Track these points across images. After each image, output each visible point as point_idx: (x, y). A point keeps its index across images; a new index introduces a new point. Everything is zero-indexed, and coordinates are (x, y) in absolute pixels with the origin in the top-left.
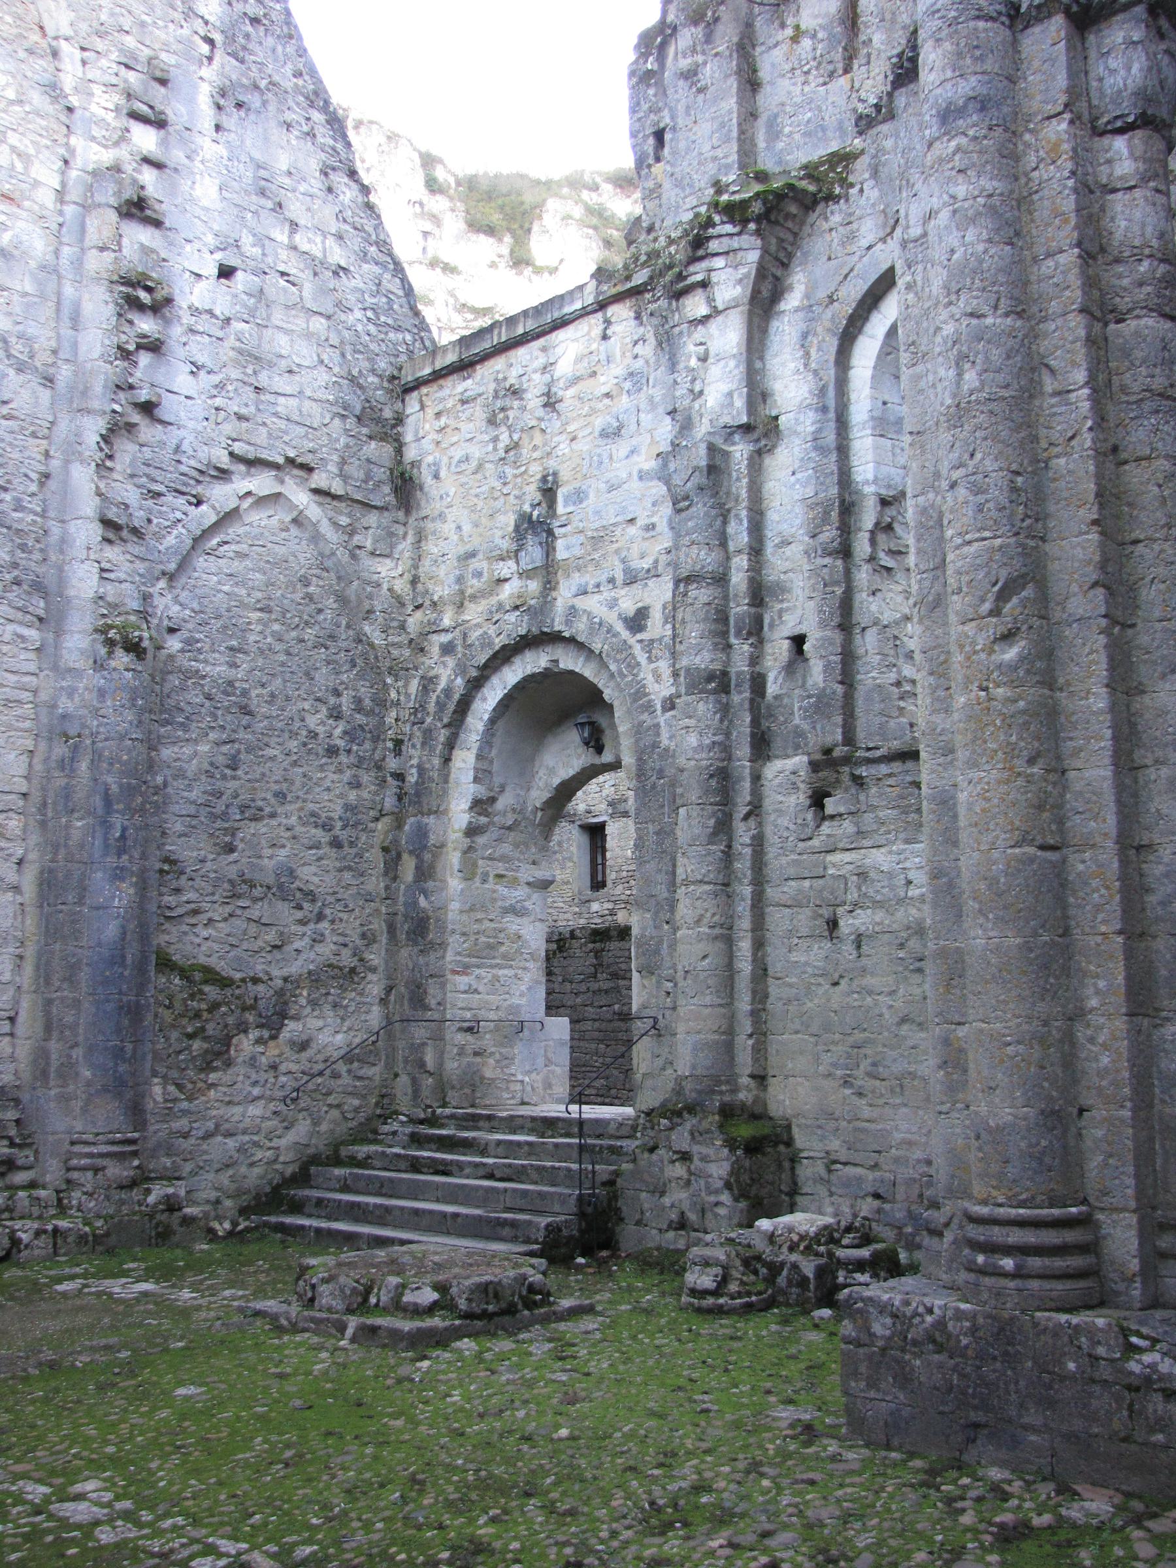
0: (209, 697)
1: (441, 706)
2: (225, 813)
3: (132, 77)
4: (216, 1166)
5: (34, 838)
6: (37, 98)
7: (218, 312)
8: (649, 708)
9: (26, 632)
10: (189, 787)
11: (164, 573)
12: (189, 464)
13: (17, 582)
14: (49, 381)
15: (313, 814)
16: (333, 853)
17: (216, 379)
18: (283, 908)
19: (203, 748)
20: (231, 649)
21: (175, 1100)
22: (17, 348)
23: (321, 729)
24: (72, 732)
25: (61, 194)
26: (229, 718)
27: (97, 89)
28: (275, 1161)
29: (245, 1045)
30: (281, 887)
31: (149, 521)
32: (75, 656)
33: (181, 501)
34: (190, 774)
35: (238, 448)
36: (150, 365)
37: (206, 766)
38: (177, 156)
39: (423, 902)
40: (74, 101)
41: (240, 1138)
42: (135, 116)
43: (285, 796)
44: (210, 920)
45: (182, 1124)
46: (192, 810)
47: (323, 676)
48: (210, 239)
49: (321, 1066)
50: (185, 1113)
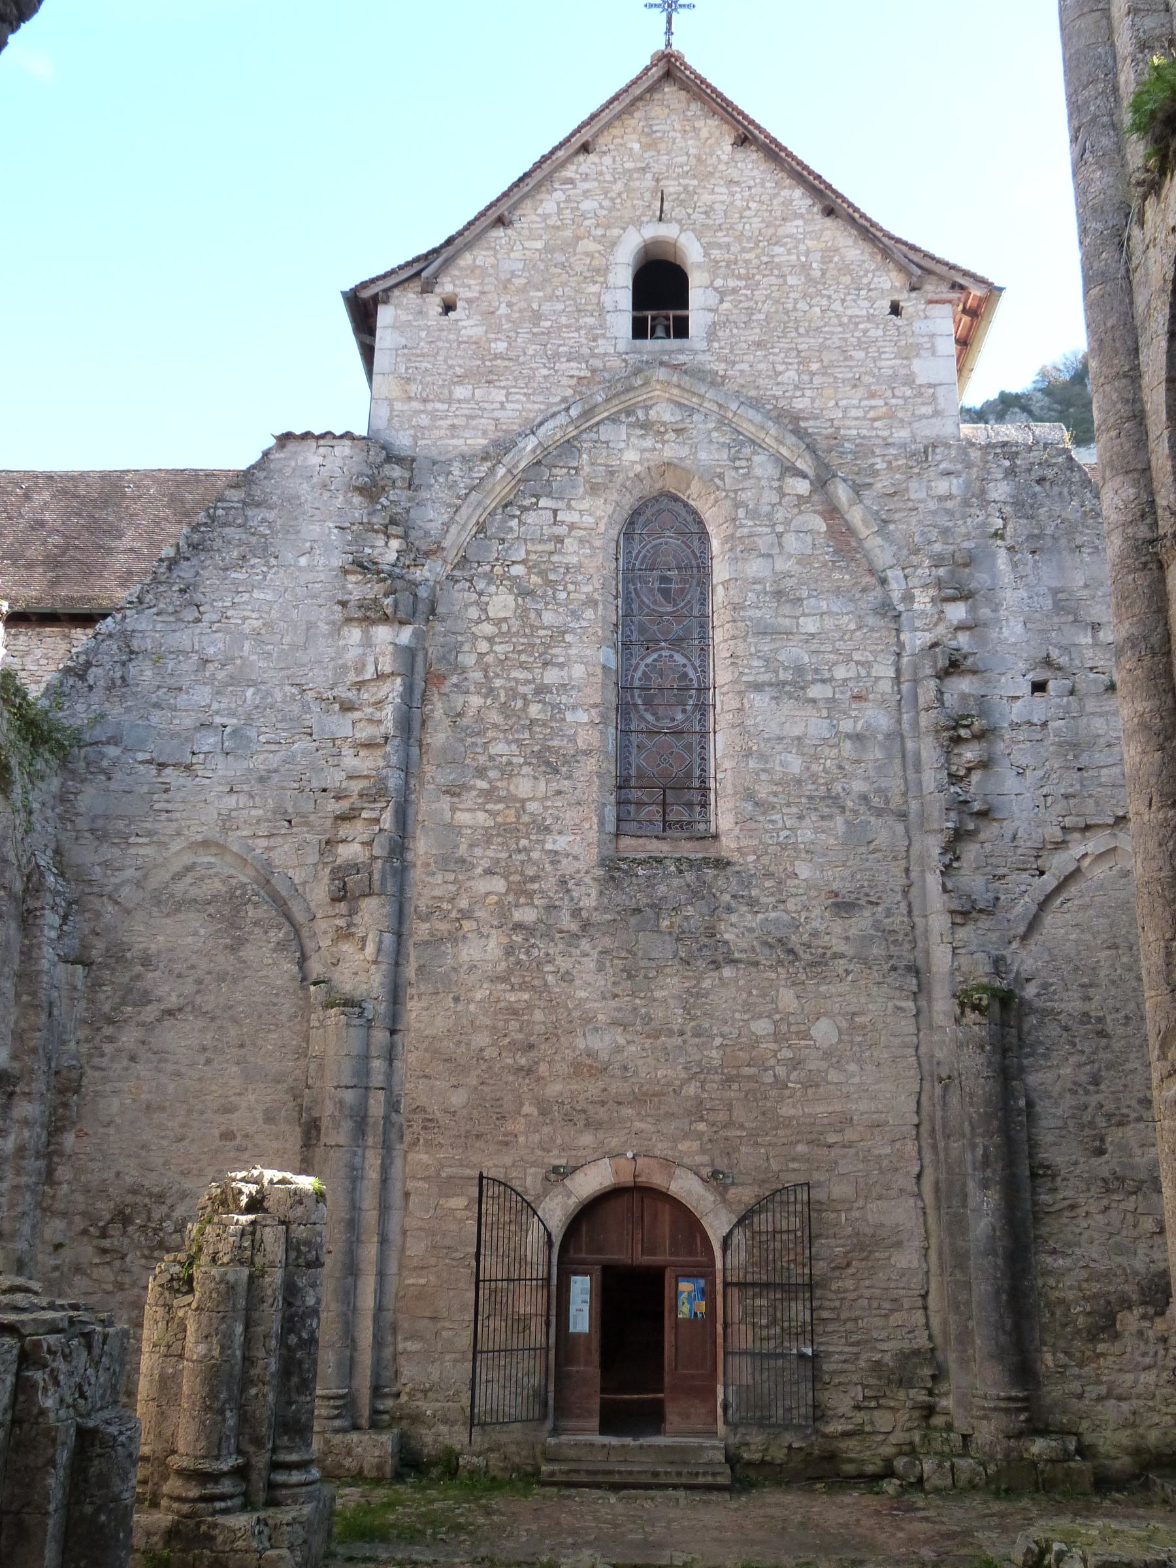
0: (1066, 1029)
3: (941, 572)
5: (928, 1156)
6: (871, 620)
7: (1035, 720)
9: (903, 1004)
10: (1056, 1104)
12: (1026, 844)
13: (894, 968)
14: (903, 816)
17: (1041, 773)
19: (1066, 1071)
20: (1082, 986)
21: (1065, 1366)
22: (876, 801)
24: (944, 1076)
25: (897, 680)
27: (917, 592)
31: (997, 899)
32: (942, 1016)
33: (1025, 875)
34: (1055, 1094)
35: (1068, 821)
36: (981, 780)
37: (1069, 1085)
38: (985, 612)
40: (901, 608)
41: (1134, 1402)
42: (946, 600)
45: (1075, 1386)
46: (1060, 1123)
48: (1022, 666)
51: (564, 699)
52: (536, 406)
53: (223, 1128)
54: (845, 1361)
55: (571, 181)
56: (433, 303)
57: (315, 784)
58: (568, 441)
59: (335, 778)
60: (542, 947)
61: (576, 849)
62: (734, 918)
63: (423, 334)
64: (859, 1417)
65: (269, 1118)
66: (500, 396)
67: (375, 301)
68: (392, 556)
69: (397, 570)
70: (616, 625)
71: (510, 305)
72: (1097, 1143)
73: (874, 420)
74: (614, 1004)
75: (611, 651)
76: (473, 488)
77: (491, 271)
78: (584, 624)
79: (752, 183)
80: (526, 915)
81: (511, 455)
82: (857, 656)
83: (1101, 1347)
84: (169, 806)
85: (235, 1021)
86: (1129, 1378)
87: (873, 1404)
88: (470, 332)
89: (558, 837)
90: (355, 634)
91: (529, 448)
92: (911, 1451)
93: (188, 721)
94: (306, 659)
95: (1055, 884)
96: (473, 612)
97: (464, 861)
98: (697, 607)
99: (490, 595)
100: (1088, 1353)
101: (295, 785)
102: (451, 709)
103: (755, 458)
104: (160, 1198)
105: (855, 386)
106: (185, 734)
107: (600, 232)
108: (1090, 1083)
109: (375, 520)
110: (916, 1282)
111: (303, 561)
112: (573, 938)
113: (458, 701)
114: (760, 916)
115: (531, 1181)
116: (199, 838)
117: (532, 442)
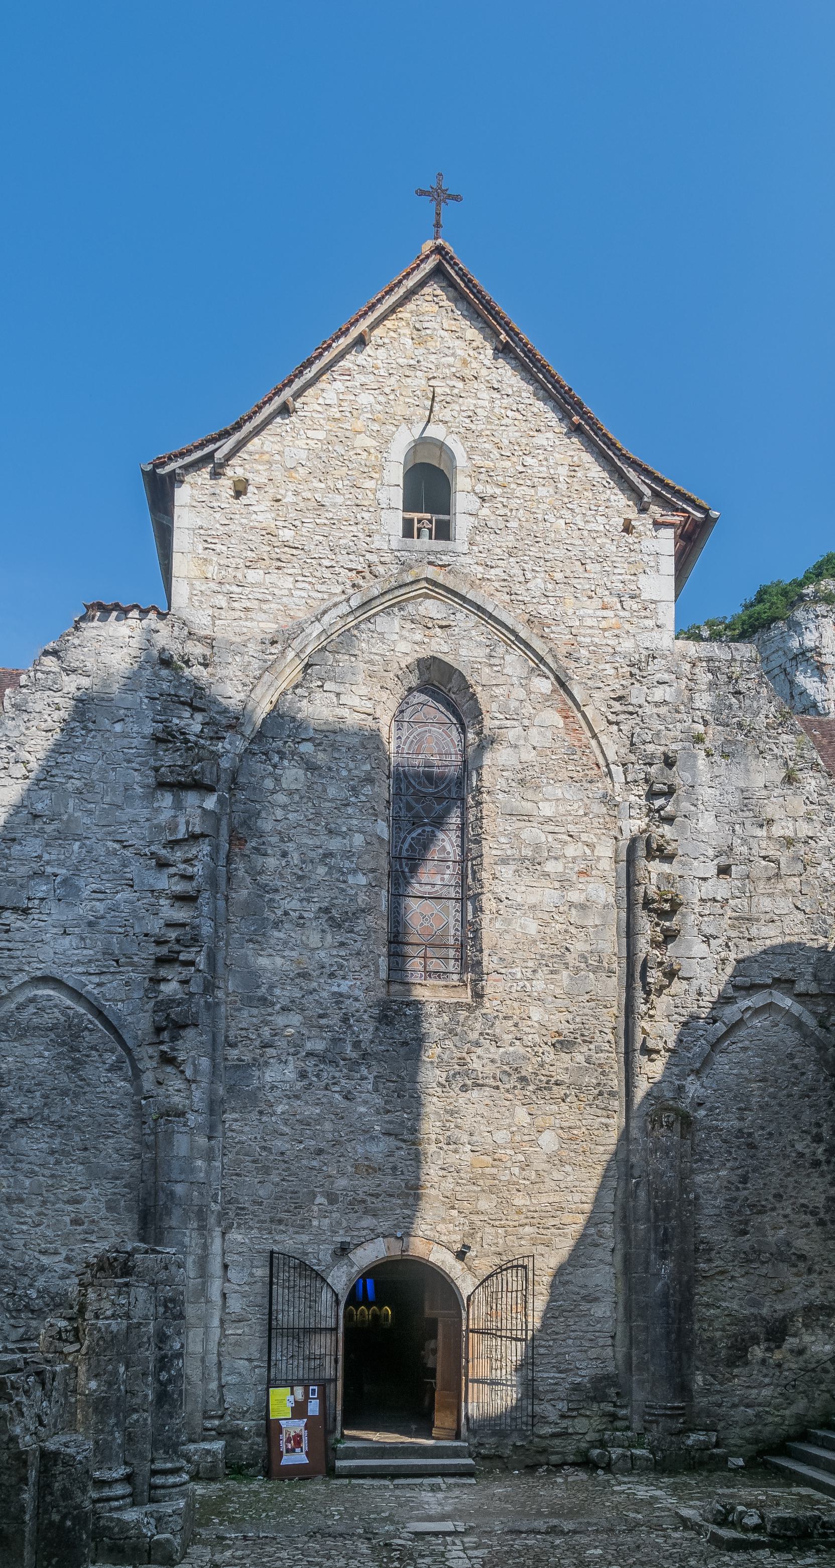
0: (725, 1141)
2: (739, 1211)
4: (741, 1424)
5: (619, 1237)
7: (719, 898)
10: (715, 1198)
11: (692, 1071)
15: (803, 1205)
16: (818, 1229)
18: (783, 1267)
20: (739, 1109)
23: (807, 1151)
26: (740, 1152)
28: (782, 1424)
29: (758, 1352)
30: (781, 1253)
32: (635, 1131)
34: (715, 1191)
38: (685, 806)
41: (757, 1408)
43: (781, 1196)
44: (732, 1277)
46: (717, 1211)
47: (808, 1116)
49: (813, 1366)
50: (718, 1392)
51: (347, 864)
52: (320, 595)
53: (73, 1215)
54: (556, 1384)
55: (348, 373)
56: (225, 485)
57: (137, 930)
58: (349, 630)
59: (155, 926)
60: (329, 1071)
61: (357, 993)
62: (479, 1051)
63: (217, 515)
64: (565, 1423)
65: (110, 1208)
66: (288, 582)
67: (174, 479)
68: (197, 728)
69: (202, 741)
70: (388, 802)
71: (296, 493)
72: (742, 1227)
73: (604, 630)
74: (387, 1117)
75: (385, 824)
76: (267, 670)
77: (277, 457)
78: (363, 798)
79: (510, 393)
80: (319, 1046)
81: (299, 639)
82: (584, 837)
83: (736, 1371)
84: (10, 945)
85: (78, 1129)
87: (575, 1413)
88: (260, 517)
89: (341, 982)
90: (167, 799)
91: (315, 634)
92: (602, 1444)
93: (23, 870)
94: (124, 818)
95: (725, 1029)
96: (269, 783)
97: (266, 999)
98: (454, 789)
99: (284, 768)
101: (121, 930)
102: (252, 869)
103: (507, 657)
104: (22, 1272)
105: (590, 597)
106: (19, 881)
107: (376, 427)
108: (740, 1182)
109: (180, 693)
110: (608, 1326)
111: (118, 727)
112: (353, 1065)
113: (259, 861)
114: (502, 1050)
115: (320, 1255)
116: (39, 974)
117: (317, 628)
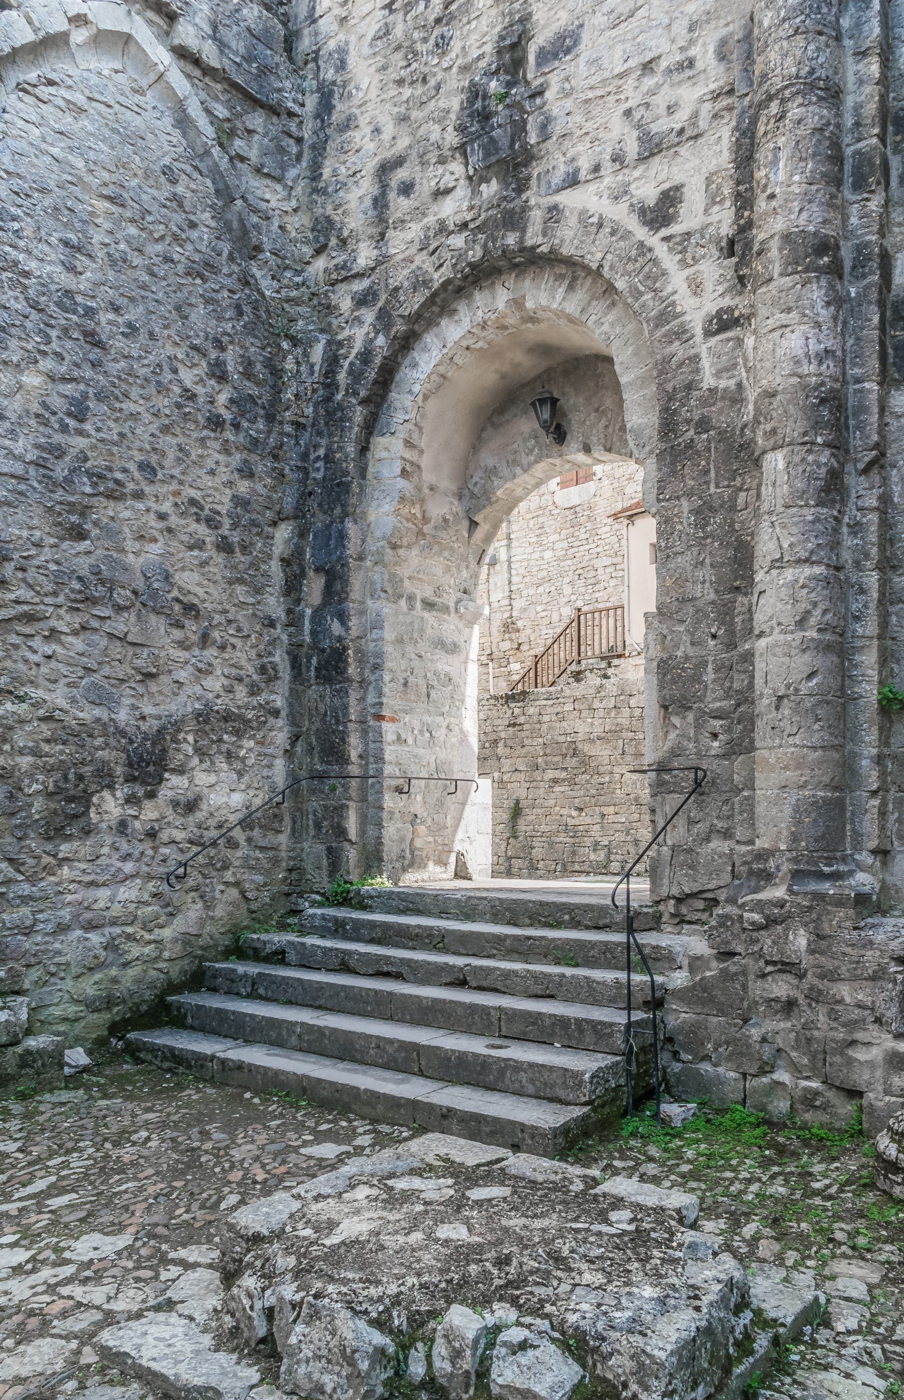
0: (35, 306)
1: (356, 375)
2: (68, 480)
8: (682, 334)
15: (193, 502)
16: (220, 558)
18: (157, 623)
19: (32, 380)
20: (66, 243)
23: (200, 390)
26: (69, 344)
29: (110, 805)
30: (154, 594)
37: (35, 407)
39: (336, 628)
43: (154, 472)
44: (53, 630)
46: (18, 468)
47: (199, 314)
49: (213, 833)
72: (74, 518)
83: (65, 849)
86: (103, 894)
100: (46, 859)
108: (69, 414)
